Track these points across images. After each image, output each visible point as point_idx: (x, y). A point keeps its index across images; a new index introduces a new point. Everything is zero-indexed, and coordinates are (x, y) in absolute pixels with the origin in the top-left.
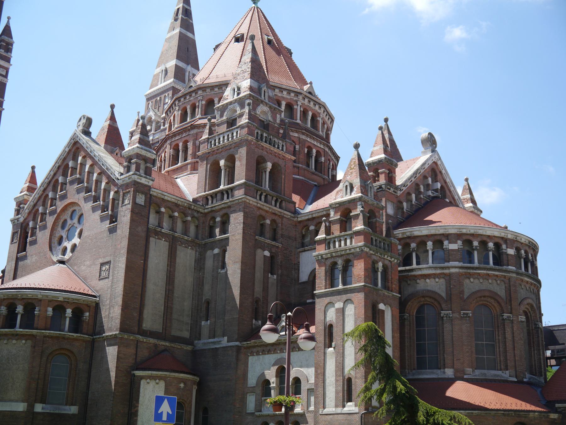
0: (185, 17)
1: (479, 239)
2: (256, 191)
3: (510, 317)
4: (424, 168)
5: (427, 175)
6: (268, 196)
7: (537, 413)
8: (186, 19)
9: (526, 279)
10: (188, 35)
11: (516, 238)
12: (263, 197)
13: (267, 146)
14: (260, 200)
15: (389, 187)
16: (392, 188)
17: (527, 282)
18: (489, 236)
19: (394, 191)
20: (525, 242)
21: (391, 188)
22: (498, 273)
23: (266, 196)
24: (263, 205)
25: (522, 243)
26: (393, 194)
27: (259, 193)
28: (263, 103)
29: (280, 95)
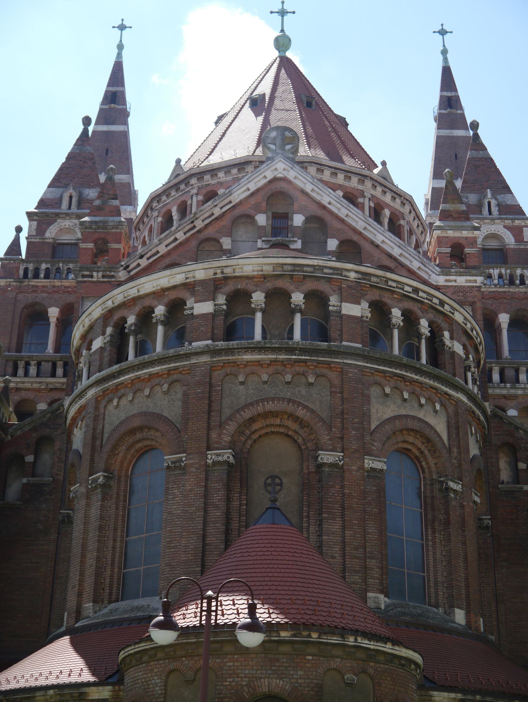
0: (445, 110)
1: (138, 308)
2: (11, 364)
3: (180, 460)
4: (230, 202)
5: (252, 212)
6: (43, 363)
7: (51, 692)
8: (449, 114)
9: (248, 357)
10: (455, 135)
11: (222, 273)
12: (33, 370)
13: (44, 284)
14: (26, 374)
15: (86, 273)
16: (98, 271)
17: (259, 363)
18: (154, 293)
19: (103, 276)
20: (262, 271)
21: (95, 274)
22: (159, 368)
23: (39, 364)
24: (23, 383)
25: (248, 278)
26: (103, 282)
27: (21, 365)
28: (60, 216)
29: (214, 182)
